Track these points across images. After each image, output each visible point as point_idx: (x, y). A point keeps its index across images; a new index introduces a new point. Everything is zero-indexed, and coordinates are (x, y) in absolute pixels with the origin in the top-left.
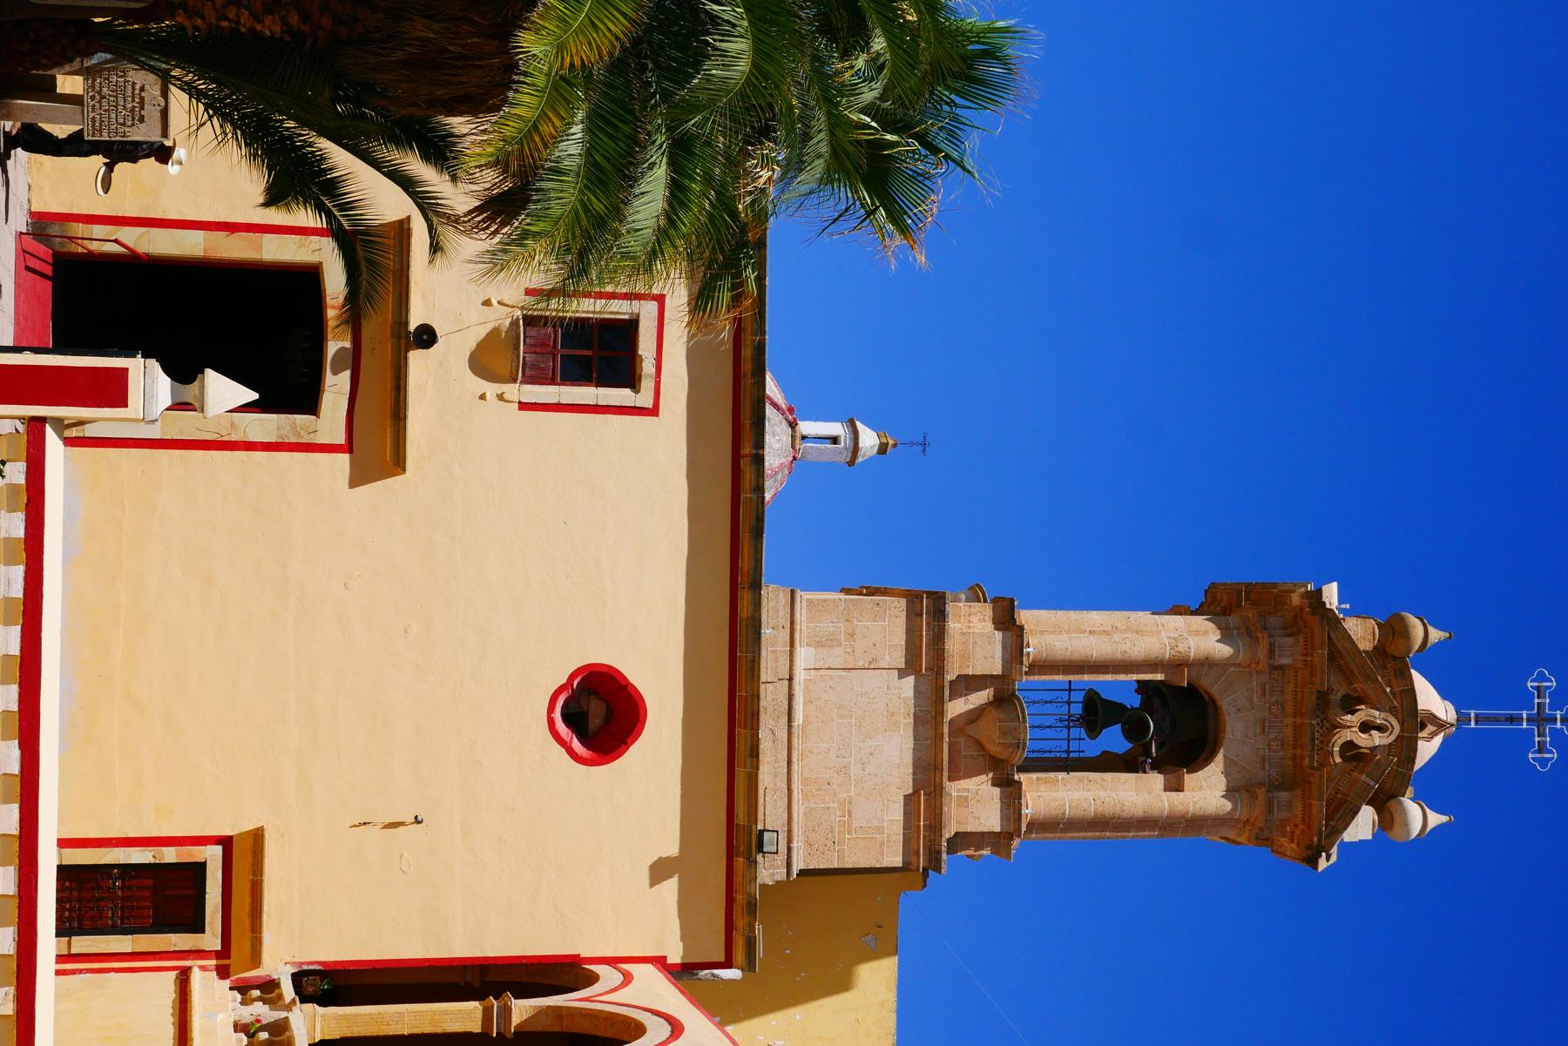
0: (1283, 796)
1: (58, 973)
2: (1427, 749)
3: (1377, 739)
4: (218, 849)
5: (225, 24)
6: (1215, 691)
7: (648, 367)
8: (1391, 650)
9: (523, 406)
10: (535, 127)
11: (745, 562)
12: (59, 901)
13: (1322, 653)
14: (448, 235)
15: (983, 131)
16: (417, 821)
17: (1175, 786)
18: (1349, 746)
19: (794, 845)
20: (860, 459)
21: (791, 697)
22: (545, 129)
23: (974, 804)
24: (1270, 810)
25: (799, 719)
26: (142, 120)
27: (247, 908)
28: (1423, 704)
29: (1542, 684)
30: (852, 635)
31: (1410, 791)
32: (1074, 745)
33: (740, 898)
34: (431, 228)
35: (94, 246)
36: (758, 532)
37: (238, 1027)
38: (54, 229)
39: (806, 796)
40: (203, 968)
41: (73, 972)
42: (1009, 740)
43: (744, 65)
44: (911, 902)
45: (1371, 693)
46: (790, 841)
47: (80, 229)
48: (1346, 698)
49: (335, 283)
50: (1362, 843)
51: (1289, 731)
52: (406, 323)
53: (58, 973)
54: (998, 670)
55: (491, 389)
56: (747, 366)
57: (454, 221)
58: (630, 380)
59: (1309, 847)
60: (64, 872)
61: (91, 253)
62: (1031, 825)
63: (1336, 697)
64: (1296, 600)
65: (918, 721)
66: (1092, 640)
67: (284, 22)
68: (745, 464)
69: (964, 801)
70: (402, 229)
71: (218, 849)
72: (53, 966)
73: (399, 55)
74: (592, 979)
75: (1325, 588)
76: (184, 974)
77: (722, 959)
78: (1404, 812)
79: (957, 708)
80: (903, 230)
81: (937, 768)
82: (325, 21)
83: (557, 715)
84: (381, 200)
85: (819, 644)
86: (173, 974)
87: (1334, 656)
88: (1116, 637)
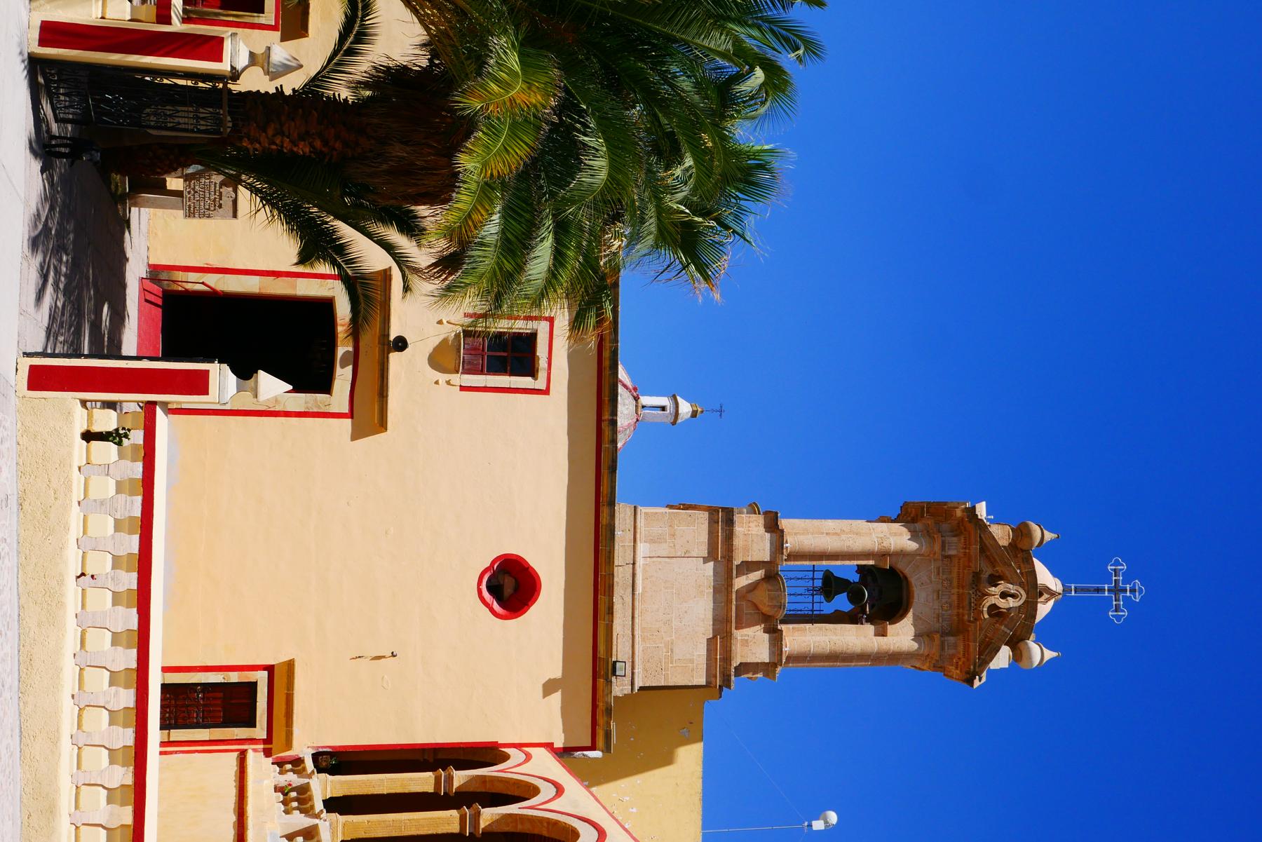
0: (951, 639)
1: (161, 753)
2: (1044, 609)
3: (1012, 603)
4: (265, 673)
5: (274, 147)
6: (907, 571)
7: (542, 363)
8: (1020, 546)
9: (463, 388)
10: (469, 216)
11: (605, 489)
12: (162, 707)
13: (976, 548)
14: (414, 280)
15: (757, 215)
16: (393, 655)
17: (884, 634)
18: (993, 607)
19: (636, 671)
20: (679, 421)
22: (476, 217)
23: (752, 644)
24: (943, 649)
25: (639, 589)
26: (220, 206)
27: (283, 711)
28: (1040, 581)
29: (1118, 567)
31: (1033, 636)
32: (816, 607)
33: (601, 705)
34: (404, 276)
35: (189, 286)
36: (613, 469)
37: (277, 789)
38: (164, 276)
39: (643, 640)
40: (255, 750)
41: (171, 753)
42: (775, 603)
43: (603, 175)
44: (712, 707)
45: (1007, 573)
46: (633, 668)
47: (180, 276)
48: (991, 576)
49: (343, 310)
50: (1002, 669)
51: (955, 597)
52: (388, 335)
53: (161, 753)
54: (767, 558)
55: (443, 378)
56: (606, 363)
57: (416, 271)
58: (530, 369)
59: (967, 673)
60: (165, 688)
61: (187, 291)
62: (789, 658)
63: (985, 576)
64: (959, 513)
65: (716, 591)
66: (828, 539)
67: (311, 145)
68: (605, 426)
69: (745, 643)
70: (386, 275)
71: (265, 673)
72: (159, 749)
73: (385, 167)
74: (506, 757)
75: (978, 506)
76: (243, 754)
77: (589, 744)
78: (1029, 649)
79: (741, 582)
80: (706, 278)
81: (728, 621)
82: (338, 145)
83: (484, 587)
84: (371, 257)
85: (651, 541)
86: (236, 754)
87: (983, 549)
88: (843, 537)
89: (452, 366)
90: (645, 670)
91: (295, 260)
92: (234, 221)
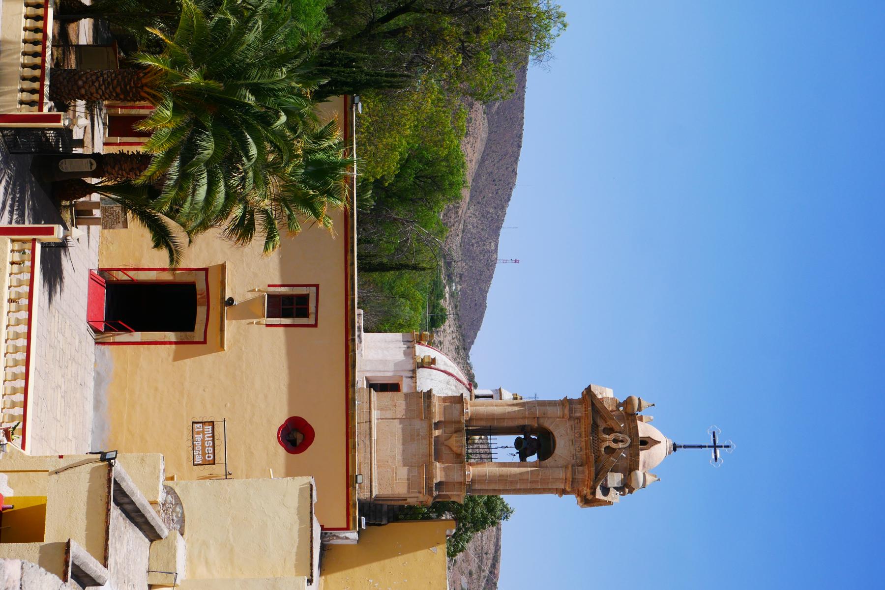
0: (581, 468)
6: (551, 428)
9: (267, 325)
11: (350, 379)
18: (608, 448)
21: (370, 428)
33: (351, 503)
39: (378, 467)
46: (371, 482)
49: (200, 286)
51: (584, 444)
56: (350, 308)
63: (601, 428)
68: (350, 343)
81: (430, 455)
85: (381, 409)
89: (260, 314)
90: (379, 484)
91: (152, 244)
92: (125, 230)
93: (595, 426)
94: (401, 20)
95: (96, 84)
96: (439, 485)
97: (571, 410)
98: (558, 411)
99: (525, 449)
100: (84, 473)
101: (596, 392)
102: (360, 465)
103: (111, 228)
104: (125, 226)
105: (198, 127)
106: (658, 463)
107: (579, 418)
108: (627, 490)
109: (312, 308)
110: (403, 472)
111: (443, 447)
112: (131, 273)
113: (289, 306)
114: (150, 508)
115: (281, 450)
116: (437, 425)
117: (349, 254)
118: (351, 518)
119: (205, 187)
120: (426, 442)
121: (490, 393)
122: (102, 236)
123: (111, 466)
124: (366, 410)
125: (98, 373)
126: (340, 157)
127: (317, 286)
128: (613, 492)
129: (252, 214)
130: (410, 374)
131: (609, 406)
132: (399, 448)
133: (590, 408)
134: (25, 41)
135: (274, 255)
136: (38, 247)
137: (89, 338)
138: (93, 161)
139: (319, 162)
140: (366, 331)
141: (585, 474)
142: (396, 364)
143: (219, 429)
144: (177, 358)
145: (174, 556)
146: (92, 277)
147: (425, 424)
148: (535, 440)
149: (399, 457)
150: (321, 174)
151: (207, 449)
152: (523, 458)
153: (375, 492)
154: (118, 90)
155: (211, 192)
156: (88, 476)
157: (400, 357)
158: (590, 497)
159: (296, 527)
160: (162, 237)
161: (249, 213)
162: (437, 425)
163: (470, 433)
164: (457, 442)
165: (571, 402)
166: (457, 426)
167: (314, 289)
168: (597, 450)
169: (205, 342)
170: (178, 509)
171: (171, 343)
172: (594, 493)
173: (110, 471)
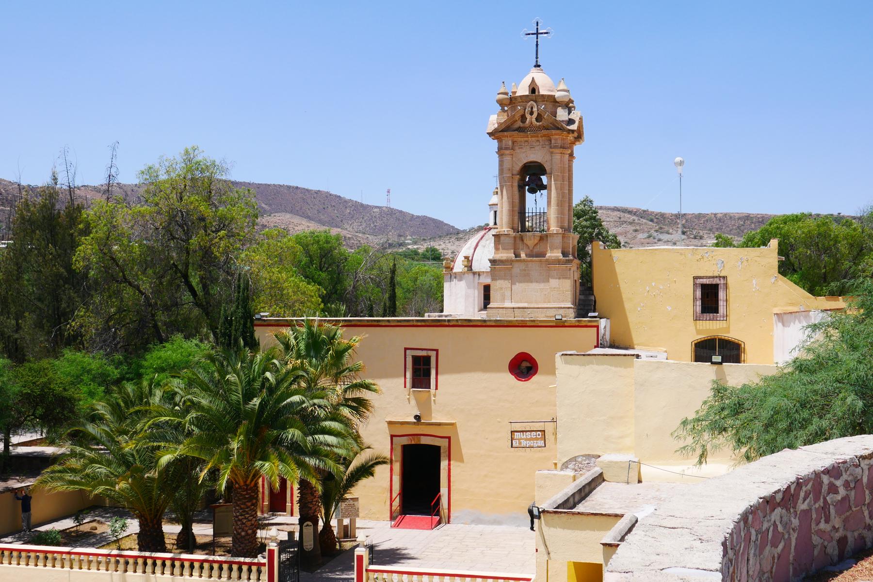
0: (553, 141)
6: (520, 165)
9: (436, 389)
18: (537, 120)
25: (526, 305)
30: (501, 288)
36: (470, 321)
49: (405, 441)
55: (433, 398)
63: (521, 125)
81: (541, 261)
85: (503, 300)
89: (425, 395)
90: (563, 301)
91: (371, 478)
93: (519, 129)
94: (195, 281)
95: (244, 521)
96: (564, 254)
97: (507, 149)
98: (507, 159)
99: (536, 185)
100: (548, 531)
101: (493, 128)
102: (547, 317)
103: (358, 510)
104: (356, 499)
105: (277, 442)
106: (550, 80)
107: (513, 142)
108: (571, 105)
109: (424, 353)
110: (554, 282)
111: (535, 250)
112: (394, 495)
113: (422, 371)
114: (578, 482)
115: (535, 378)
116: (517, 255)
117: (380, 324)
118: (590, 324)
119: (326, 436)
120: (530, 264)
121: (492, 213)
122: (364, 518)
123: (544, 511)
124: (504, 311)
125: (473, 522)
126: (304, 330)
127: (406, 349)
128: (572, 116)
129: (347, 400)
130: (477, 276)
131: (504, 118)
132: (534, 285)
133: (505, 133)
134: (210, 576)
135: (381, 384)
136: (372, 567)
137: (444, 528)
138: (305, 524)
139: (307, 346)
140: (442, 311)
141: (557, 138)
142: (469, 287)
143: (517, 427)
144: (461, 460)
145: (616, 463)
146: (397, 526)
147: (516, 265)
148: (531, 177)
149: (542, 286)
150: (316, 345)
151: (532, 436)
152: (544, 187)
153: (570, 305)
154: (249, 504)
155: (330, 432)
156: (552, 529)
157: (463, 284)
158: (576, 134)
159: (595, 367)
160: (366, 471)
161: (346, 403)
162: (517, 255)
163: (524, 229)
164: (531, 239)
165: (500, 149)
166: (518, 240)
167: (408, 351)
168: (540, 128)
169: (449, 438)
170: (580, 460)
171: (449, 465)
172: (573, 131)
173: (548, 512)
